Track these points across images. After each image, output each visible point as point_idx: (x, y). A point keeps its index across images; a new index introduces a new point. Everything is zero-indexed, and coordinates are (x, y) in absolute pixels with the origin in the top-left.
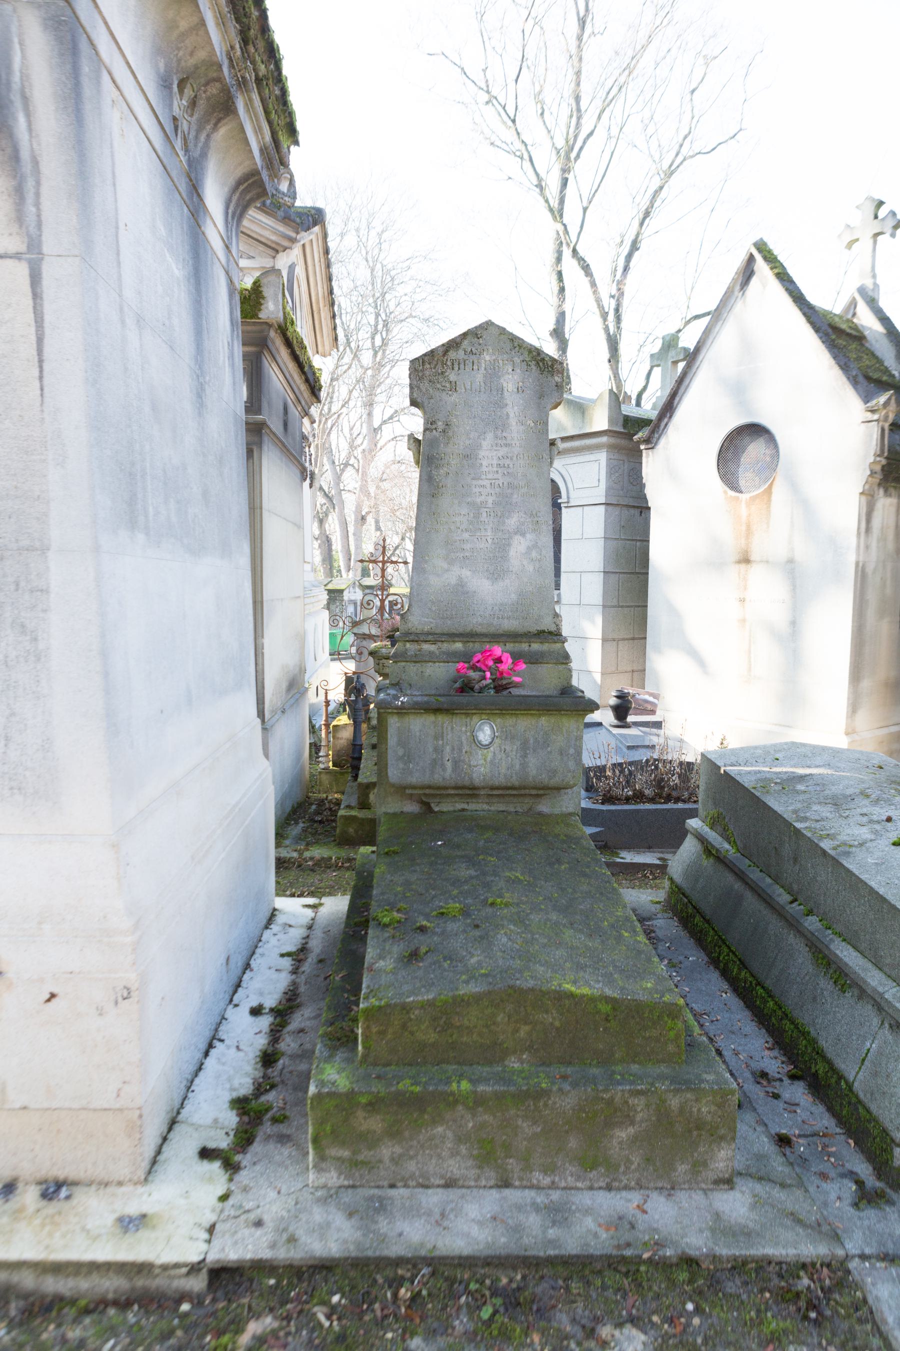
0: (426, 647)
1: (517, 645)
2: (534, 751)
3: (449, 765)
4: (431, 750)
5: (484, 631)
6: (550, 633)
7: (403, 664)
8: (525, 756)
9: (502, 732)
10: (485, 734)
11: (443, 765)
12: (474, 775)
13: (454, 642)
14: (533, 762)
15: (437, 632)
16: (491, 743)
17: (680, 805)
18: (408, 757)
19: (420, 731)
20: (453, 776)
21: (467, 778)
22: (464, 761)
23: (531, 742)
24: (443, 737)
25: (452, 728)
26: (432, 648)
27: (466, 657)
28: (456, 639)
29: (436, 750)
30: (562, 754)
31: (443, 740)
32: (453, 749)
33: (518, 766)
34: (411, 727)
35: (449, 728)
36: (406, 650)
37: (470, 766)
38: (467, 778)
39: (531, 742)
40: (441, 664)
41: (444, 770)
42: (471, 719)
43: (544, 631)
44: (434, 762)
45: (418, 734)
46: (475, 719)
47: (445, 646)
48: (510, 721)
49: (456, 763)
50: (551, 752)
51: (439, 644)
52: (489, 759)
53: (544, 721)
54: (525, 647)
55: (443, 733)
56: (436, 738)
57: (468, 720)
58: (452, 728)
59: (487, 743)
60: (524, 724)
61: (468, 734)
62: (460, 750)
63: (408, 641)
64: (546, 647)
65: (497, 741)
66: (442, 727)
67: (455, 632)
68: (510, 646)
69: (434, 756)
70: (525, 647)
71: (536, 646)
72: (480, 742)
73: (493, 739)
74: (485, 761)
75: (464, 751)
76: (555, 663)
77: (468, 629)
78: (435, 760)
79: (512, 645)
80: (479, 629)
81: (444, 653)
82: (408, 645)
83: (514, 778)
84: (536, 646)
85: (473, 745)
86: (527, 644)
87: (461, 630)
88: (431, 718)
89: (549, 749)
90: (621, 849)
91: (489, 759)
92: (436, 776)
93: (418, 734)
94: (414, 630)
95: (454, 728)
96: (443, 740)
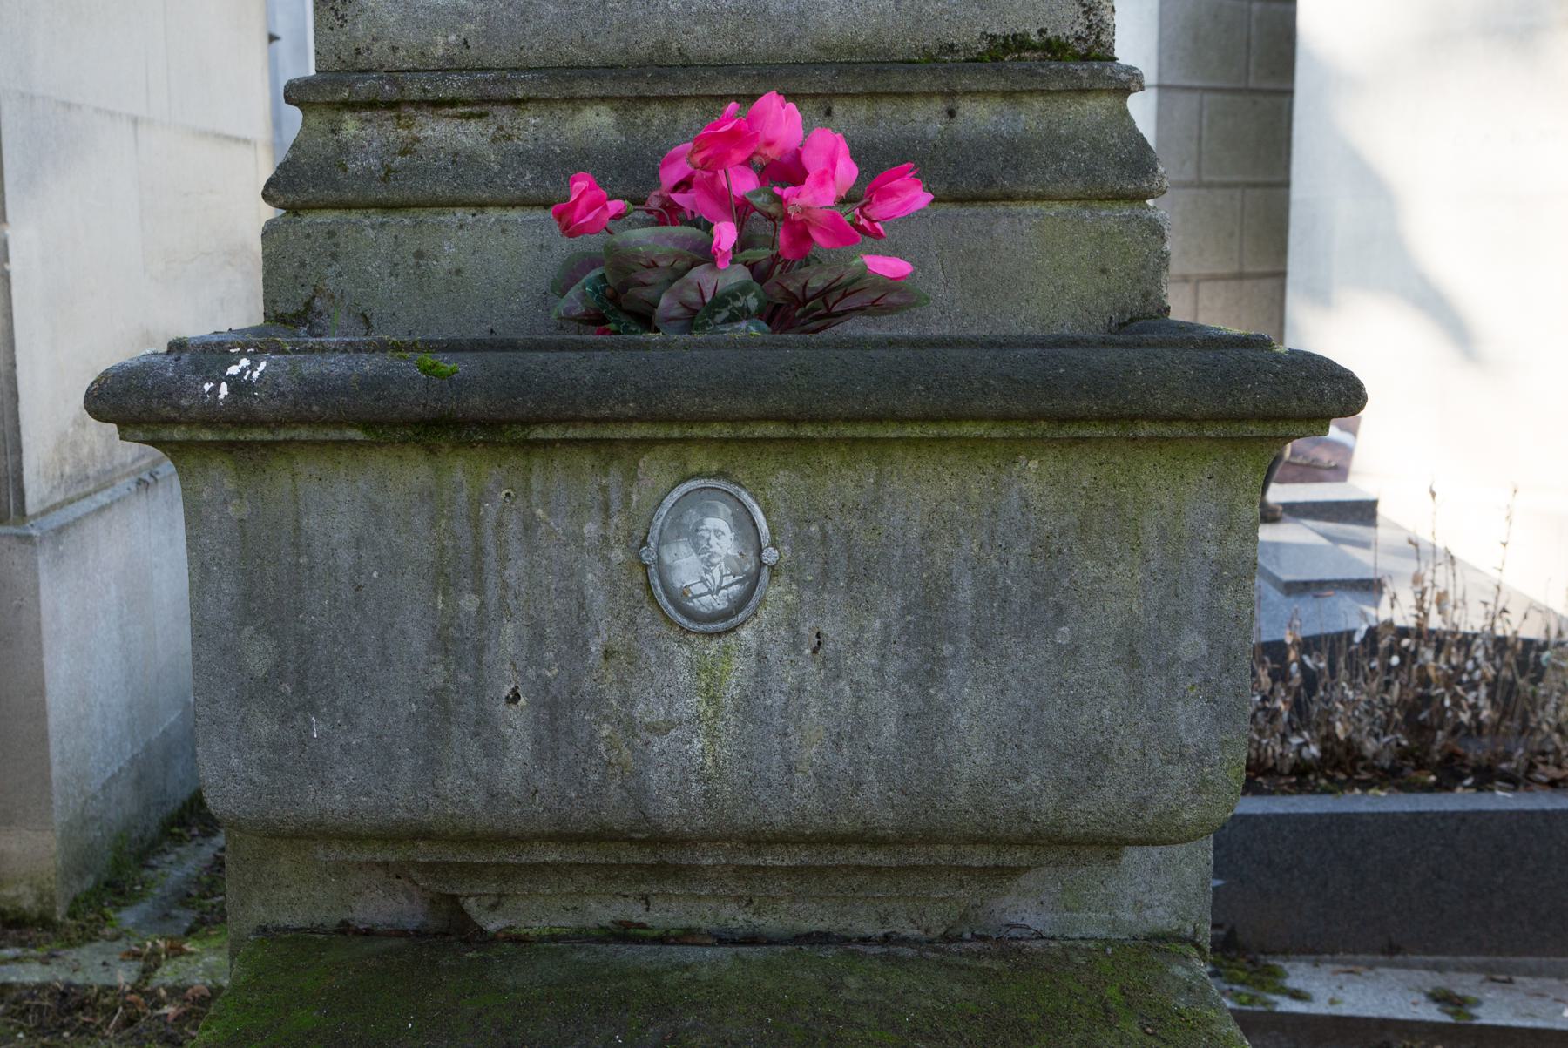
0: (437, 130)
1: (886, 108)
2: (982, 644)
3: (517, 723)
4: (419, 643)
5: (723, 48)
6: (1054, 49)
7: (330, 216)
8: (930, 672)
9: (802, 540)
10: (707, 556)
11: (483, 724)
12: (655, 777)
13: (575, 102)
14: (974, 704)
15: (492, 59)
16: (740, 603)
17: (1502, 799)
18: (301, 687)
19: (358, 542)
20: (543, 781)
21: (614, 792)
22: (596, 702)
23: (965, 593)
24: (478, 572)
25: (529, 526)
26: (469, 135)
27: (630, 171)
28: (585, 88)
29: (444, 642)
30: (1133, 661)
31: (479, 590)
32: (538, 637)
33: (890, 728)
34: (310, 522)
35: (514, 526)
36: (343, 148)
37: (629, 727)
38: (614, 792)
39: (965, 593)
40: (515, 214)
41: (494, 749)
42: (631, 476)
43: (1018, 43)
44: (439, 707)
45: (345, 558)
46: (653, 471)
47: (531, 126)
48: (843, 483)
49: (556, 713)
50: (1075, 650)
51: (504, 115)
52: (731, 690)
53: (1032, 477)
54: (925, 118)
55: (480, 551)
56: (443, 578)
57: (614, 478)
58: (529, 526)
59: (719, 602)
60: (921, 500)
61: (618, 555)
62: (576, 642)
63: (349, 106)
64: (1029, 117)
65: (775, 593)
66: (476, 522)
67: (581, 56)
68: (851, 117)
69: (438, 676)
70: (925, 118)
71: (981, 116)
72: (679, 599)
73: (752, 582)
74: (712, 699)
75: (595, 647)
76: (1084, 199)
77: (645, 45)
78: (439, 697)
79: (862, 111)
80: (699, 40)
81: (525, 158)
82: (351, 126)
83: (874, 787)
84: (981, 116)
85: (645, 614)
86: (938, 105)
87: (609, 48)
88: (406, 475)
89: (1064, 635)
90: (1285, 952)
91: (731, 690)
92: (451, 782)
93: (345, 558)
94: (379, 53)
95: (539, 524)
96: (479, 590)
